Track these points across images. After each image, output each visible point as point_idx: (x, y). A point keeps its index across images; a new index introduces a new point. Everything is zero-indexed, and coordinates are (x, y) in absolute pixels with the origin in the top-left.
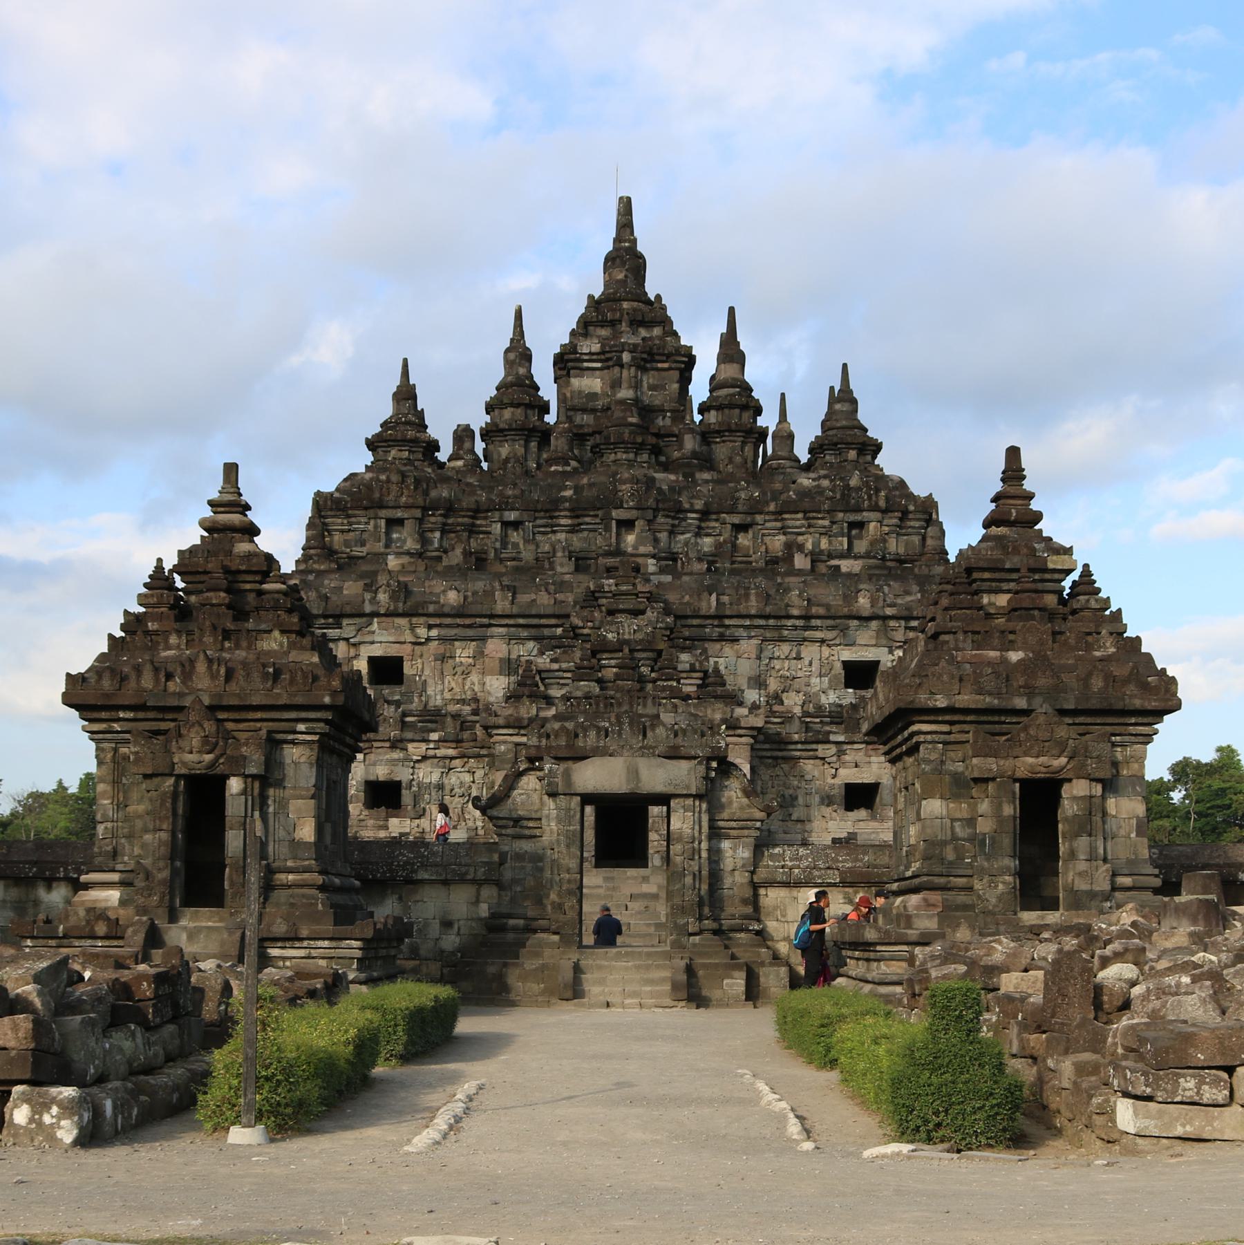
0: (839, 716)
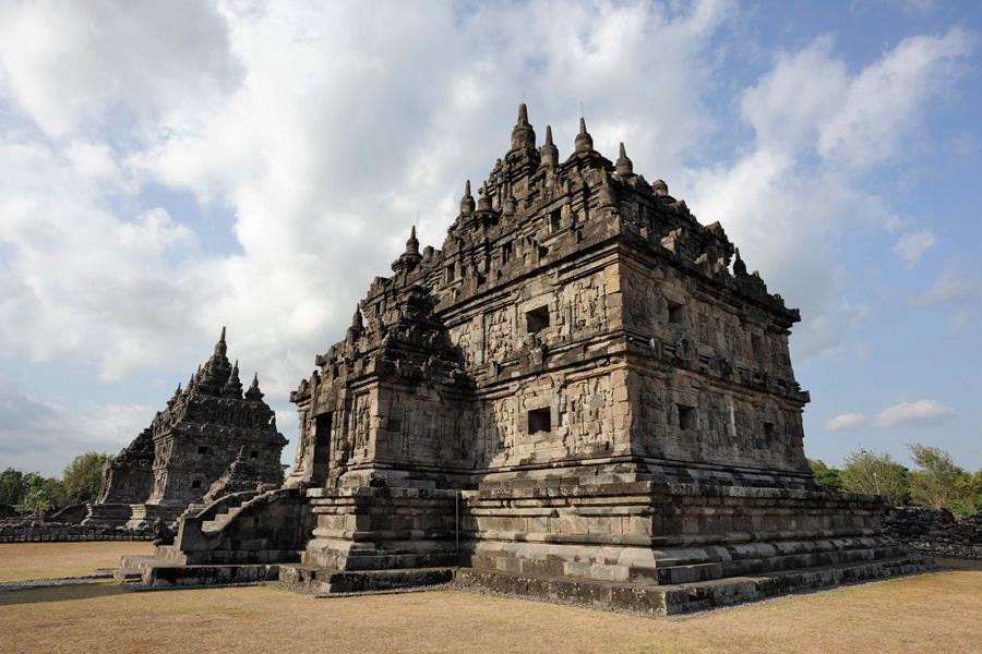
0: (520, 358)
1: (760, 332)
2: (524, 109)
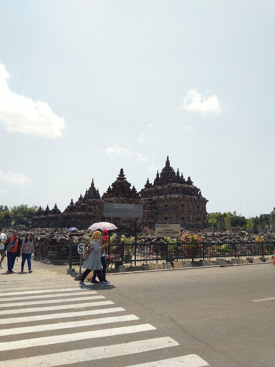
1: (200, 205)
2: (168, 157)
